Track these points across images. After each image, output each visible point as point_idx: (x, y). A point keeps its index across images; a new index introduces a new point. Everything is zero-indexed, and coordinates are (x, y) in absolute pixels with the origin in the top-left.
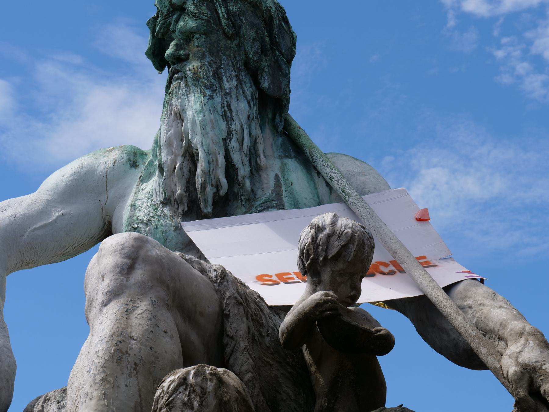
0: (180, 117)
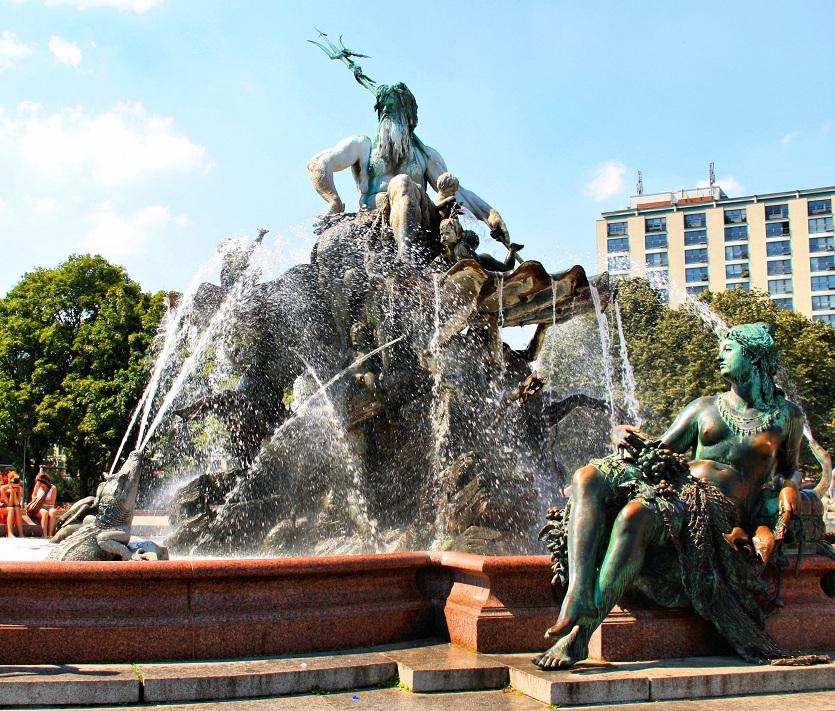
0: (388, 131)
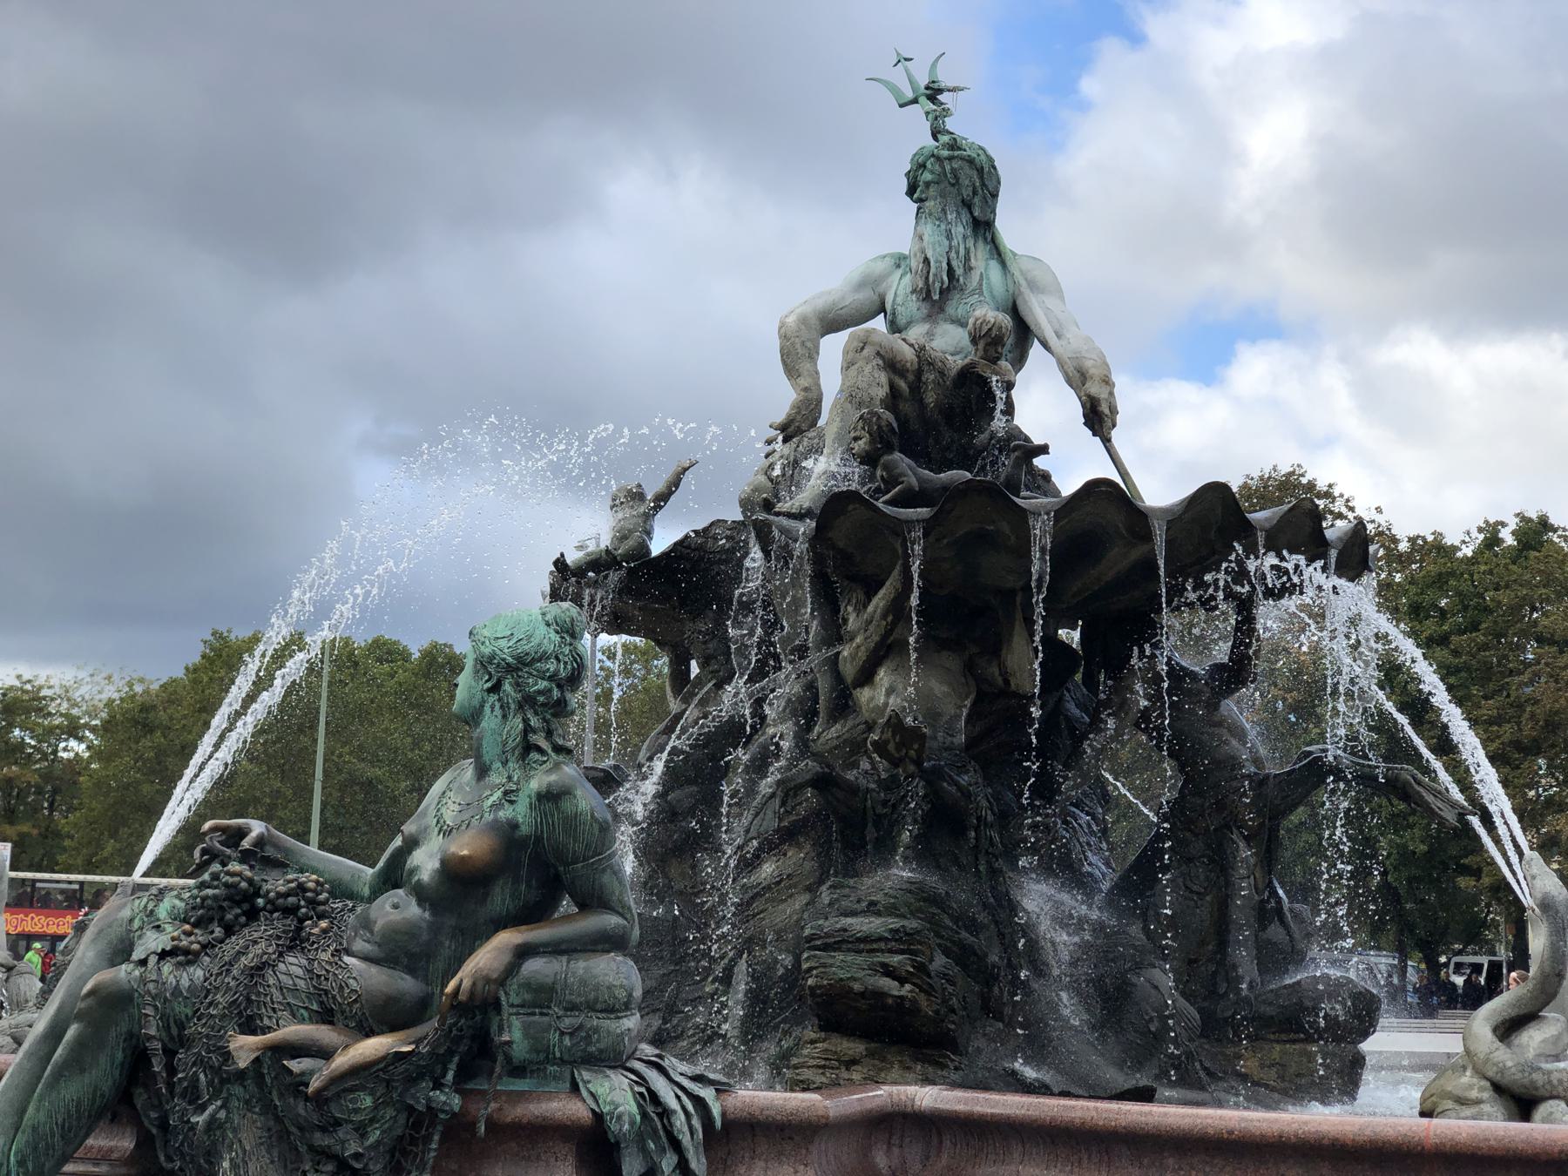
0: (921, 238)
